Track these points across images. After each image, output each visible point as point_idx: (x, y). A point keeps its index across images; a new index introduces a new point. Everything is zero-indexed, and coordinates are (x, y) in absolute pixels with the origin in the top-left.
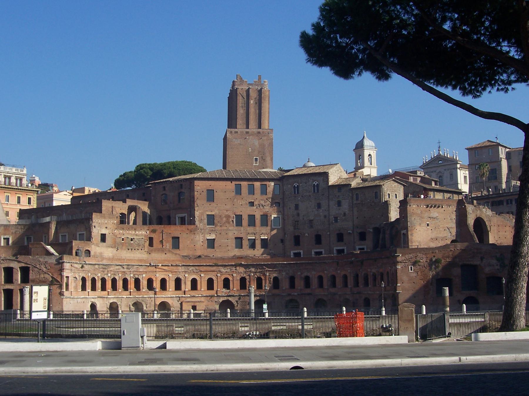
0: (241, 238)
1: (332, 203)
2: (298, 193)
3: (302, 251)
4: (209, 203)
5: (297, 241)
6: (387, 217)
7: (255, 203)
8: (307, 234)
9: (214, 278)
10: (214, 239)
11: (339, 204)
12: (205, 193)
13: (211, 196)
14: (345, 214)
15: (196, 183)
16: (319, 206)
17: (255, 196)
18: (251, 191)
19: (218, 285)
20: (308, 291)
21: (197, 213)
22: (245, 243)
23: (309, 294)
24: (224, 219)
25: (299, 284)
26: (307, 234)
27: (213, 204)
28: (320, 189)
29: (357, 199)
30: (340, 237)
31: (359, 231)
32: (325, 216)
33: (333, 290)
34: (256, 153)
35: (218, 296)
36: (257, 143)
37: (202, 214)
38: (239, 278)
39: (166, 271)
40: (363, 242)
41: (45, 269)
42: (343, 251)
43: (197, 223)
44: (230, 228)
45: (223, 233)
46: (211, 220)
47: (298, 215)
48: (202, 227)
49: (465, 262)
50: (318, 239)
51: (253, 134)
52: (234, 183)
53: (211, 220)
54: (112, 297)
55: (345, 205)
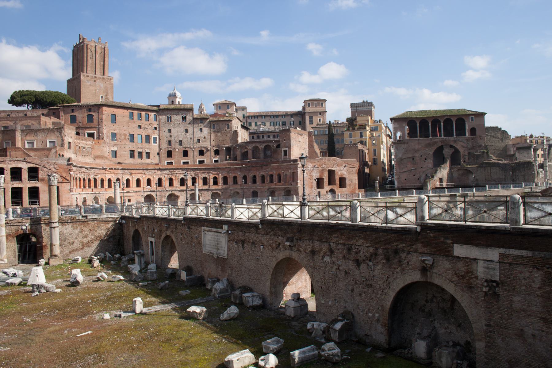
0: (133, 151)
1: (197, 130)
2: (171, 121)
3: (173, 162)
4: (113, 124)
5: (170, 154)
6: (237, 141)
7: (142, 127)
8: (178, 150)
9: (141, 178)
10: (116, 151)
11: (201, 130)
12: (110, 117)
13: (114, 118)
14: (205, 138)
15: (104, 108)
16: (187, 131)
17: (142, 122)
19: (143, 183)
20: (206, 187)
21: (105, 131)
22: (136, 154)
23: (207, 190)
24: (123, 137)
26: (178, 150)
30: (201, 153)
31: (215, 149)
32: (191, 138)
34: (102, 92)
35: (144, 192)
36: (102, 85)
37: (108, 132)
38: (157, 179)
39: (111, 173)
41: (54, 170)
42: (203, 162)
43: (105, 138)
44: (127, 143)
45: (122, 147)
46: (114, 135)
47: (171, 136)
48: (108, 142)
50: (185, 154)
51: (100, 78)
52: (129, 111)
53: (114, 135)
54: (110, 193)
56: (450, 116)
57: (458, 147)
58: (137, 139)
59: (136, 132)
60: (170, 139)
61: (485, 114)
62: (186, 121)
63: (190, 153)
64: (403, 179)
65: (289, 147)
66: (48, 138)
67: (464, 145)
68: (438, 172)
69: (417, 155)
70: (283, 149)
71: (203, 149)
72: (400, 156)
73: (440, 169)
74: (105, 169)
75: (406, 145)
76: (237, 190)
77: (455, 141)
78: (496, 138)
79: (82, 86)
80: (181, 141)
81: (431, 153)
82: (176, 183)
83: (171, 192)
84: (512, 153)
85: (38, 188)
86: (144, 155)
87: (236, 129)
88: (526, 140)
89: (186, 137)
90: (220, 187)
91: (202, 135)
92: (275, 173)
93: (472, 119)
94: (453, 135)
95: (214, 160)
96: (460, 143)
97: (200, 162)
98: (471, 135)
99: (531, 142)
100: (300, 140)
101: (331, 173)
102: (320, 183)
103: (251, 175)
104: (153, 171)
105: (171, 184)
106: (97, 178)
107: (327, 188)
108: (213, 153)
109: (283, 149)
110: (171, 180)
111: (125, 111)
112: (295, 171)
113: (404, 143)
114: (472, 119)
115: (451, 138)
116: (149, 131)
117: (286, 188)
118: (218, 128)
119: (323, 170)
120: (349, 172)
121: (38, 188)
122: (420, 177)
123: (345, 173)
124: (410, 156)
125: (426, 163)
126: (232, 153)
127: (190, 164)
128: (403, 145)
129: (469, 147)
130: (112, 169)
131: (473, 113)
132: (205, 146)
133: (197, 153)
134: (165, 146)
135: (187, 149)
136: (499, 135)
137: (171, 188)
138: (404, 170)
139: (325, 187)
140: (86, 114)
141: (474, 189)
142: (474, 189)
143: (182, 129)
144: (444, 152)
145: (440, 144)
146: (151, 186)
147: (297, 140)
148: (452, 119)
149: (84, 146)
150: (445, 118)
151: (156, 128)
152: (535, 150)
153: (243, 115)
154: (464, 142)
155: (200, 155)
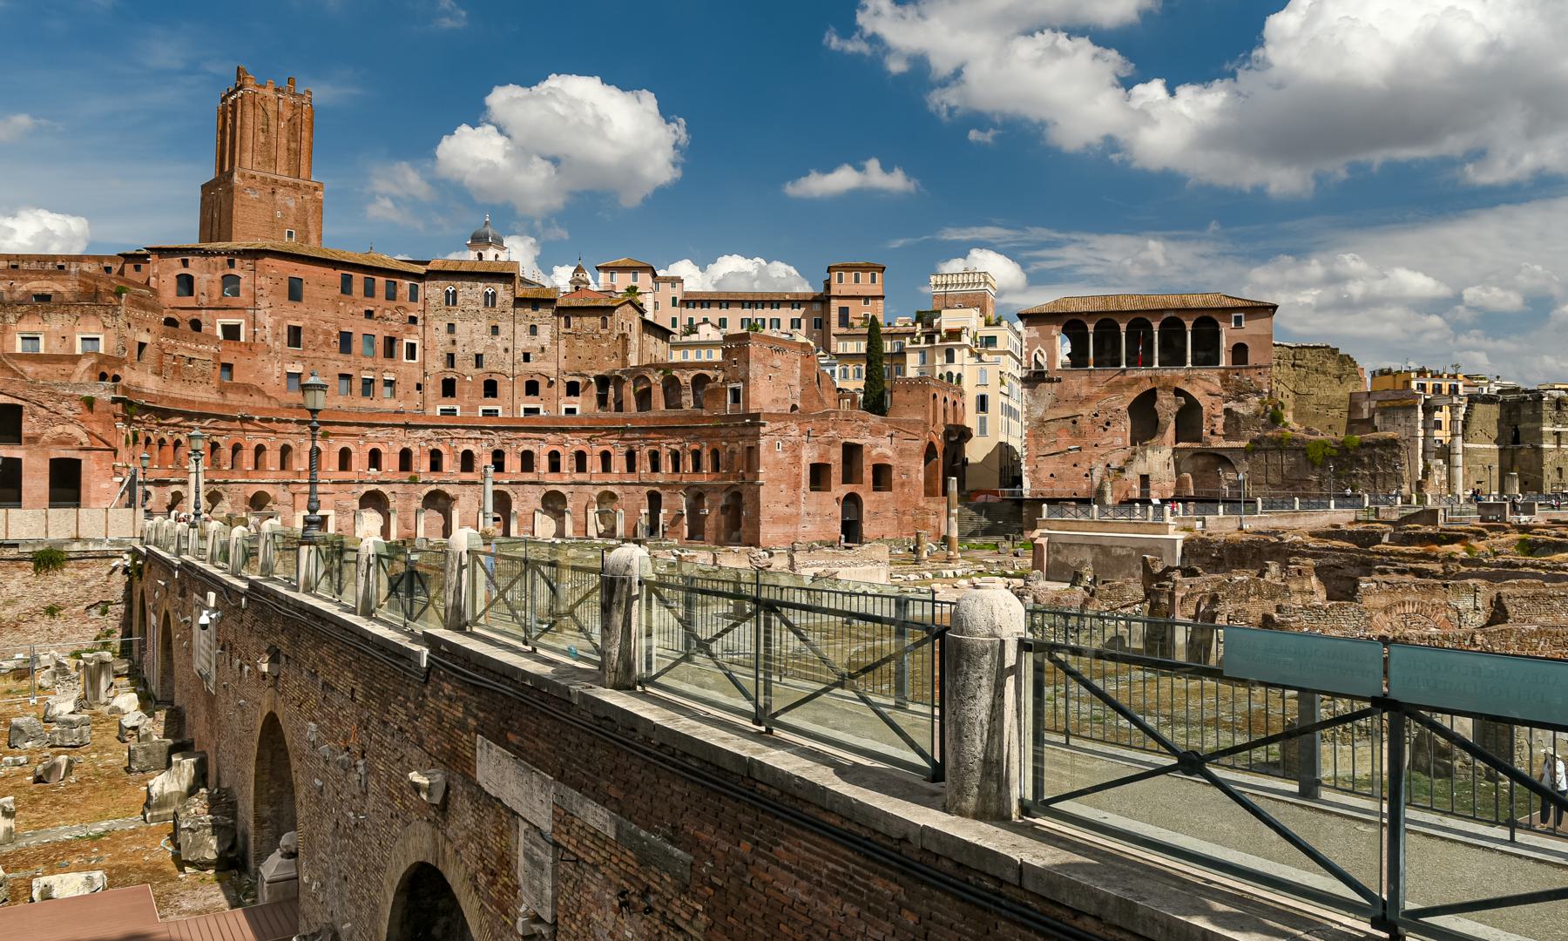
1: (520, 328)
2: (455, 303)
3: (458, 408)
5: (449, 388)
7: (376, 314)
9: (352, 448)
11: (533, 330)
13: (295, 291)
16: (495, 330)
17: (376, 301)
18: (369, 291)
19: (359, 461)
20: (529, 477)
23: (531, 483)
25: (513, 464)
27: (301, 307)
28: (498, 301)
29: (568, 325)
30: (532, 388)
31: (569, 379)
32: (506, 350)
33: (580, 477)
34: (291, 221)
36: (292, 204)
37: (279, 323)
38: (398, 450)
40: (573, 398)
42: (536, 411)
45: (318, 363)
47: (454, 342)
51: (285, 185)
52: (340, 272)
53: (295, 335)
55: (545, 334)
56: (1177, 310)
57: (1196, 395)
58: (357, 344)
59: (359, 328)
60: (451, 349)
61: (1275, 307)
62: (494, 305)
63: (503, 389)
64: (1044, 476)
65: (746, 380)
66: (79, 329)
67: (1213, 389)
71: (536, 378)
73: (1144, 451)
74: (249, 420)
76: (610, 488)
77: (1188, 380)
78: (1324, 373)
79: (237, 202)
80: (479, 357)
81: (1124, 407)
82: (450, 464)
83: (433, 487)
84: (1366, 415)
85: (19, 460)
86: (357, 385)
87: (626, 330)
88: (1408, 383)
89: (493, 346)
90: (567, 479)
91: (535, 344)
95: (564, 407)
96: (1201, 383)
97: (527, 411)
99: (1423, 387)
100: (777, 363)
101: (852, 453)
102: (819, 476)
104: (388, 430)
105: (436, 465)
106: (219, 440)
108: (563, 390)
110: (436, 457)
111: (330, 271)
112: (753, 444)
113: (1051, 381)
115: (1181, 373)
116: (395, 327)
117: (732, 486)
120: (901, 453)
121: (19, 460)
123: (890, 453)
124: (1069, 413)
126: (611, 390)
127: (500, 414)
130: (270, 421)
131: (1240, 304)
132: (543, 370)
133: (520, 388)
134: (437, 366)
135: (494, 377)
136: (1332, 366)
137: (434, 477)
138: (1048, 451)
139: (833, 487)
140: (220, 274)
141: (1221, 508)
142: (1221, 508)
143: (484, 325)
144: (1157, 406)
145: (1148, 387)
146: (379, 469)
147: (769, 362)
149: (188, 355)
150: (1165, 316)
151: (413, 320)
152: (1429, 409)
153: (674, 299)
155: (568, 394)
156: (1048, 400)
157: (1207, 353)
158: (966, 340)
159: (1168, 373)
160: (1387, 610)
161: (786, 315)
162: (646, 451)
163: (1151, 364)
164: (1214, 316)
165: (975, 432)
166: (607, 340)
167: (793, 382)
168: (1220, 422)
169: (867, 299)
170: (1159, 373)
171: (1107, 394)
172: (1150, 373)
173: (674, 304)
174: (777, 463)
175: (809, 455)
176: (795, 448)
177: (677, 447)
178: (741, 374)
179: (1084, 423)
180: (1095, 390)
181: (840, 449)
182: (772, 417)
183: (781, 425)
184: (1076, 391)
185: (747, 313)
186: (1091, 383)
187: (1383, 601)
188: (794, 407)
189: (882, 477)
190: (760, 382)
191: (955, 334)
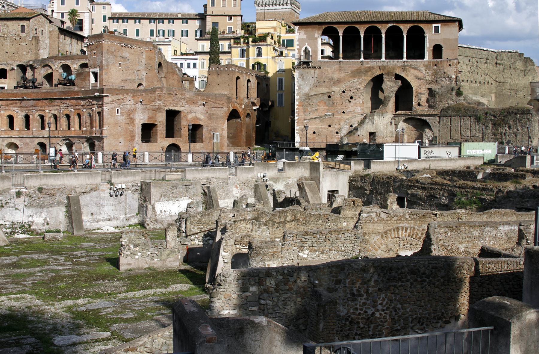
49: (170, 108)
57: (409, 79)
65: (101, 67)
67: (420, 75)
68: (367, 121)
69: (337, 90)
70: (91, 70)
72: (306, 90)
75: (317, 71)
76: (13, 141)
77: (404, 68)
78: (515, 69)
81: (362, 87)
92: (72, 111)
93: (437, 29)
94: (402, 58)
96: (412, 71)
98: (433, 59)
100: (126, 54)
101: (172, 116)
102: (148, 131)
103: (37, 114)
107: (163, 142)
109: (91, 70)
113: (314, 68)
114: (437, 29)
115: (398, 63)
118: (6, 30)
119: (157, 110)
120: (210, 117)
122: (340, 130)
123: (202, 117)
124: (325, 90)
125: (352, 104)
128: (312, 71)
129: (429, 78)
131: (438, 18)
136: (520, 65)
138: (312, 116)
139: (159, 140)
145: (378, 73)
148: (402, 26)
153: (105, 17)
154: (420, 71)
156: (312, 81)
157: (416, 52)
158: (269, 40)
159: (392, 63)
160: (384, 234)
161: (178, 26)
162: (36, 115)
163: (380, 58)
164: (421, 25)
165: (277, 104)
166: (25, 40)
167: (140, 68)
168: (424, 98)
169: (230, 17)
170: (385, 64)
171: (353, 77)
172: (380, 64)
173: (105, 20)
174: (116, 124)
175: (141, 118)
176: (130, 113)
177: (56, 112)
178: (98, 63)
179: (336, 97)
180: (343, 75)
181: (164, 114)
182: (113, 91)
183: (119, 97)
184: (330, 76)
185: (153, 26)
186: (341, 70)
187: (380, 228)
188: (140, 85)
189: (195, 131)
190: (111, 67)
191: (263, 38)
